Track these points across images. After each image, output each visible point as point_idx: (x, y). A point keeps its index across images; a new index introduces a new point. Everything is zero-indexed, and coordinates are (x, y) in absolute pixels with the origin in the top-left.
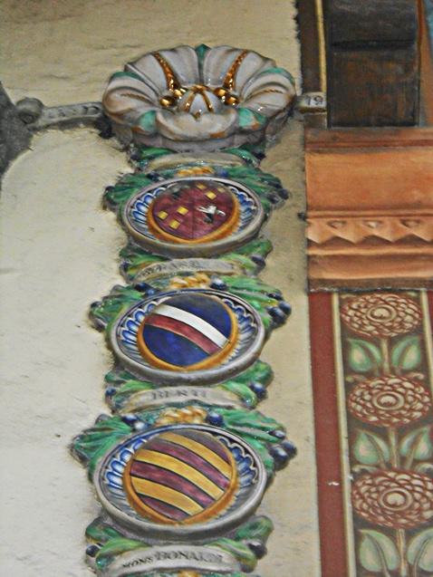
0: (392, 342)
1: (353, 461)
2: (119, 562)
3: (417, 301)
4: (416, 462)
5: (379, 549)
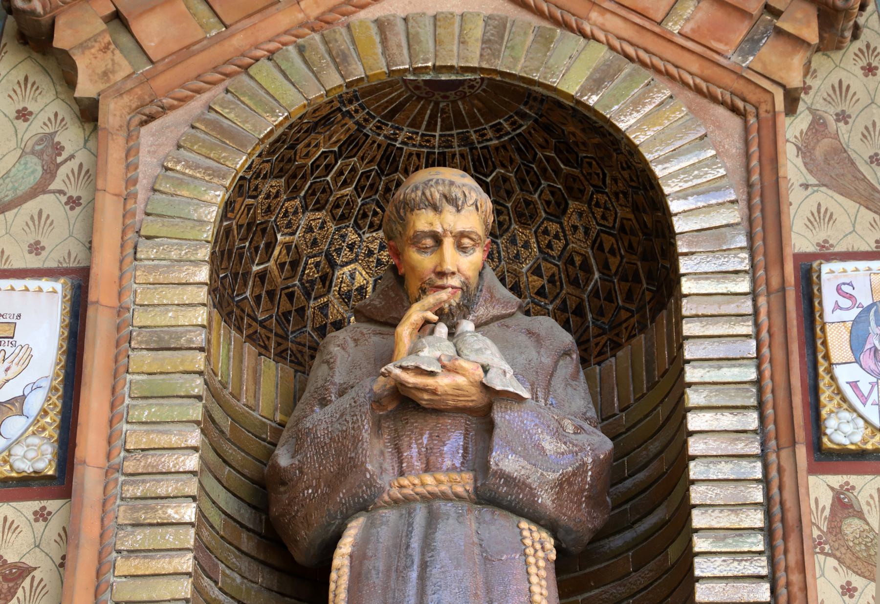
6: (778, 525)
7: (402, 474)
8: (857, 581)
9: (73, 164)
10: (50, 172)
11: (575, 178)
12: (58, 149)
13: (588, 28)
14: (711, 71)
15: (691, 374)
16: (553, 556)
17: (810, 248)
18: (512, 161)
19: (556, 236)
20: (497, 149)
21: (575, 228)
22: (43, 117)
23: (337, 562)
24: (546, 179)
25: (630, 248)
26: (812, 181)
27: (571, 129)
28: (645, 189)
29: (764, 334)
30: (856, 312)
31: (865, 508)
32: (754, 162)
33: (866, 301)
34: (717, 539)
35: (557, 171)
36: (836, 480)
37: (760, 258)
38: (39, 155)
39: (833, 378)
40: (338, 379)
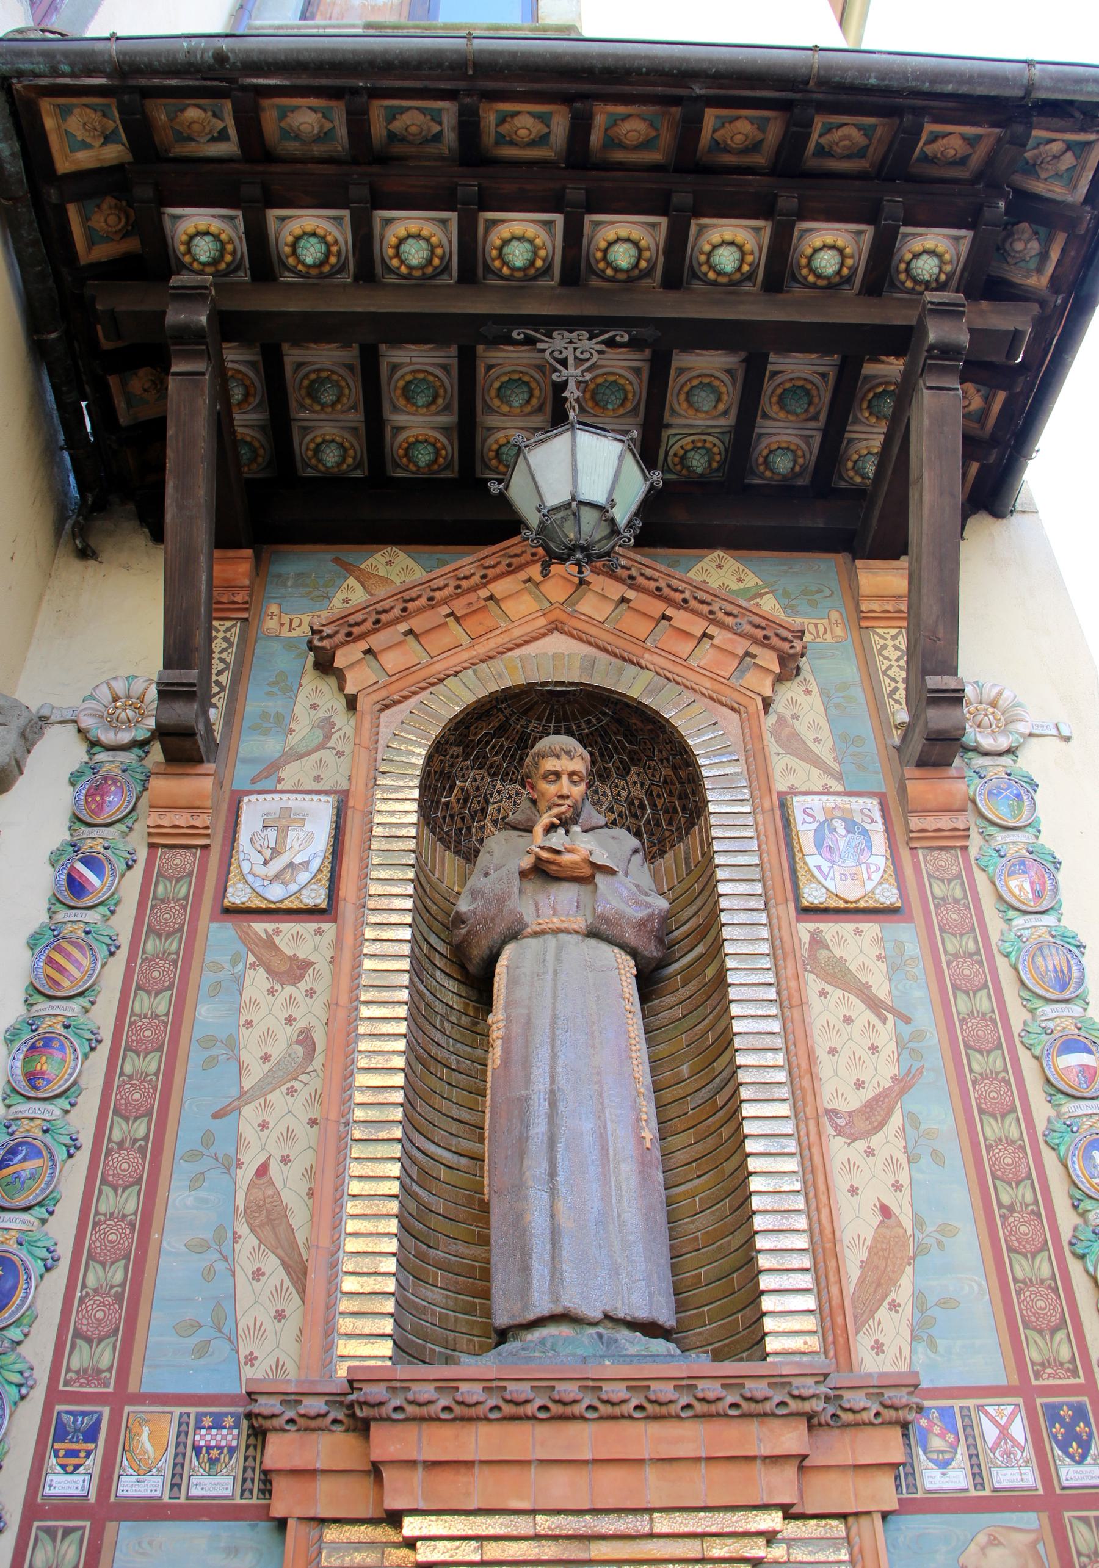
0: (178, 880)
1: (144, 952)
2: (35, 1008)
3: (195, 854)
4: (170, 954)
5: (142, 1002)
6: (779, 952)
7: (538, 916)
8: (829, 988)
9: (341, 733)
10: (328, 737)
11: (635, 752)
12: (333, 725)
13: (643, 663)
14: (717, 687)
15: (718, 860)
16: (635, 971)
17: (785, 789)
18: (596, 743)
19: (623, 789)
20: (587, 735)
21: (635, 783)
22: (325, 708)
23: (498, 970)
24: (617, 753)
25: (671, 794)
26: (781, 751)
27: (634, 721)
28: (681, 754)
29: (762, 837)
30: (816, 824)
31: (830, 943)
32: (748, 739)
33: (822, 819)
34: (740, 961)
35: (624, 748)
36: (812, 926)
37: (756, 792)
38: (322, 728)
39: (805, 863)
40: (495, 861)
